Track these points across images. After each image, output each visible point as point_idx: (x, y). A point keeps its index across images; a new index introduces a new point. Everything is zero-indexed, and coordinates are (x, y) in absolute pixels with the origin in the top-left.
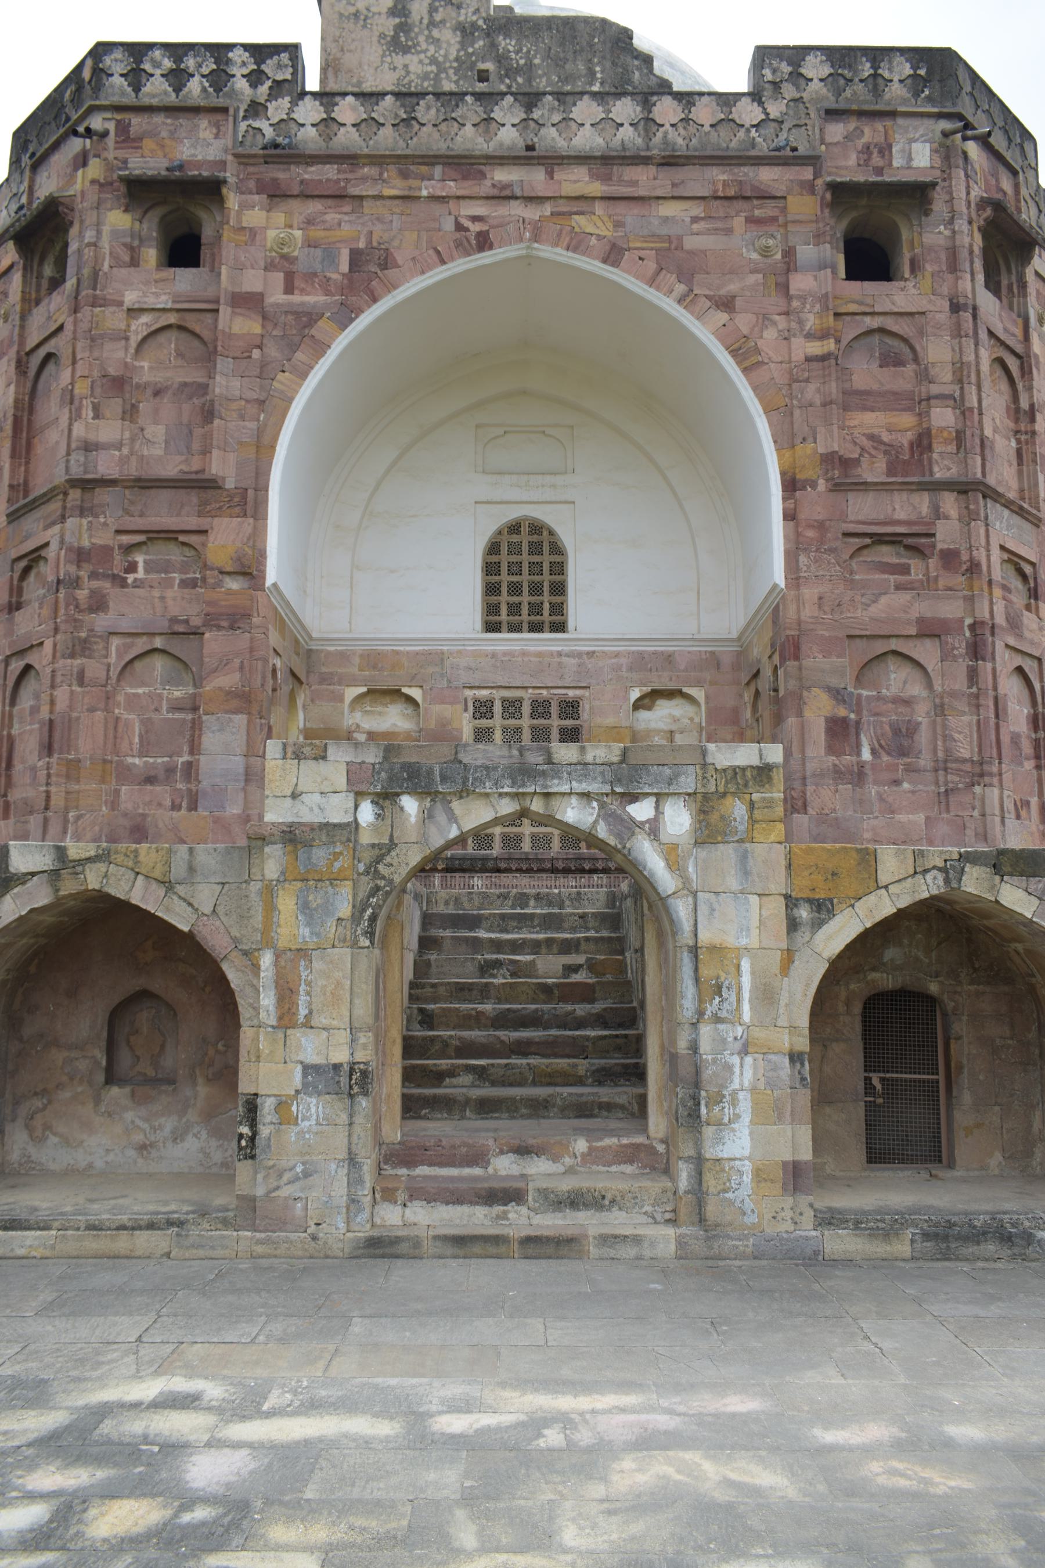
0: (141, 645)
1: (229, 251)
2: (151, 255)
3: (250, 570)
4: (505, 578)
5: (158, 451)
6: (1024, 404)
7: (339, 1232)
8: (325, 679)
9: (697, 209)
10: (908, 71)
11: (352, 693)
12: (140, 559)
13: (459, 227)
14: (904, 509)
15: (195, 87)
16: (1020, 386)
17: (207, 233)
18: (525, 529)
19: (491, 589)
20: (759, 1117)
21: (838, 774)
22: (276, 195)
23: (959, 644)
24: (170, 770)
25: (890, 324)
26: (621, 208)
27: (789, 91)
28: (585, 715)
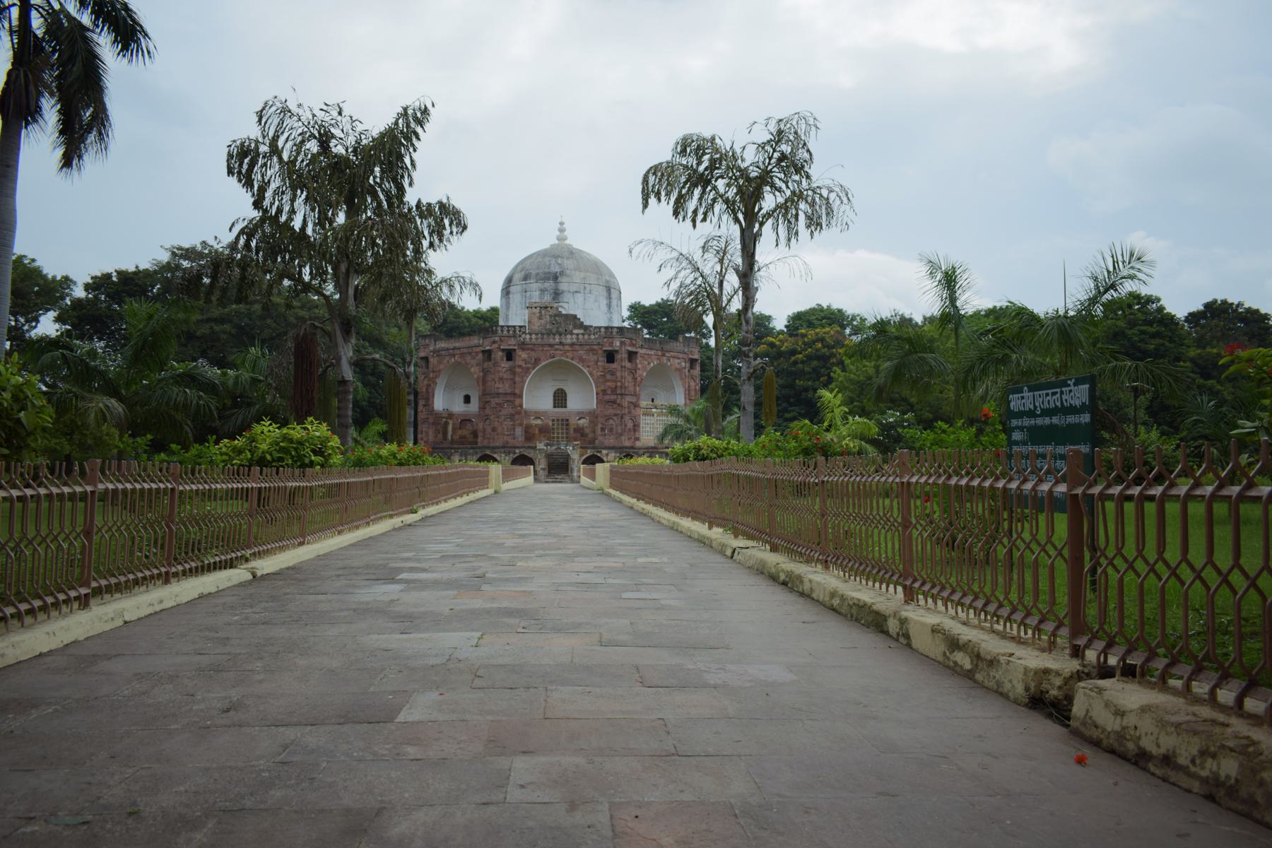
3: (521, 406)
14: (613, 397)
22: (523, 349)
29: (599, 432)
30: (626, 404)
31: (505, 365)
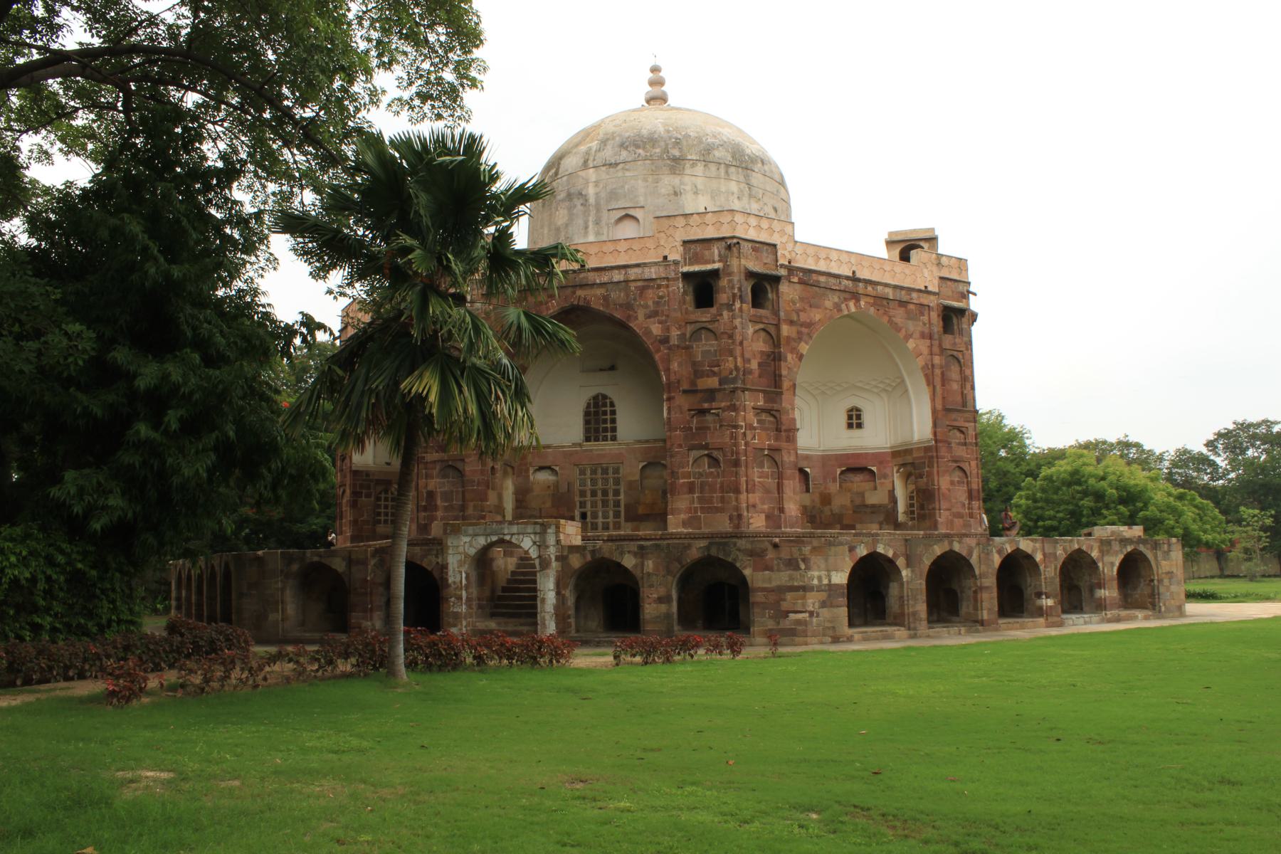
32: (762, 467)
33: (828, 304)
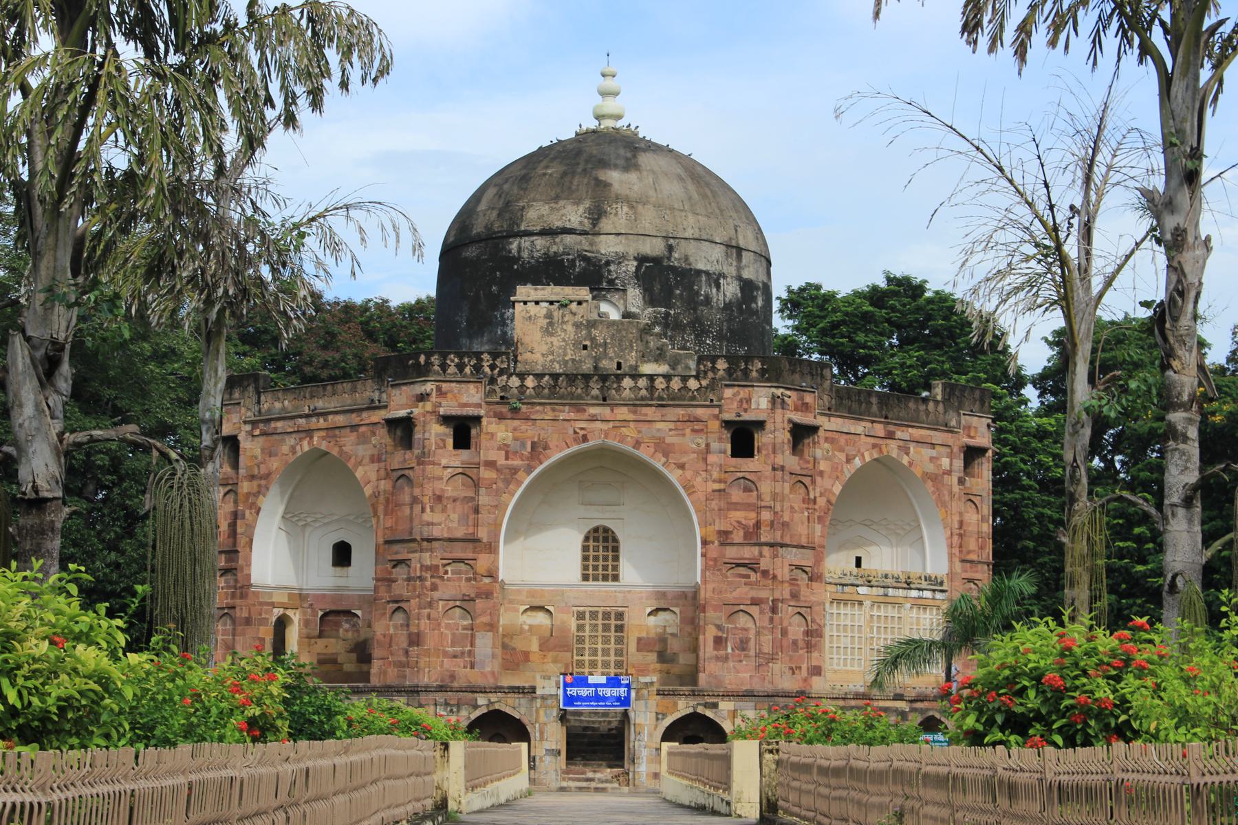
0: (451, 604)
1: (484, 443)
2: (450, 441)
3: (492, 574)
4: (591, 572)
5: (455, 525)
6: (812, 496)
7: (555, 785)
8: (511, 602)
9: (672, 426)
10: (760, 366)
11: (523, 608)
12: (449, 568)
13: (575, 432)
14: (749, 553)
15: (468, 370)
16: (811, 489)
17: (473, 432)
18: (601, 530)
19: (585, 558)
20: (648, 762)
21: (717, 658)
23: (766, 608)
24: (463, 653)
25: (747, 475)
26: (641, 425)
27: (710, 375)
28: (626, 620)
29: (707, 648)
30: (783, 572)
31: (452, 458)
32: (225, 625)
33: (285, 449)
